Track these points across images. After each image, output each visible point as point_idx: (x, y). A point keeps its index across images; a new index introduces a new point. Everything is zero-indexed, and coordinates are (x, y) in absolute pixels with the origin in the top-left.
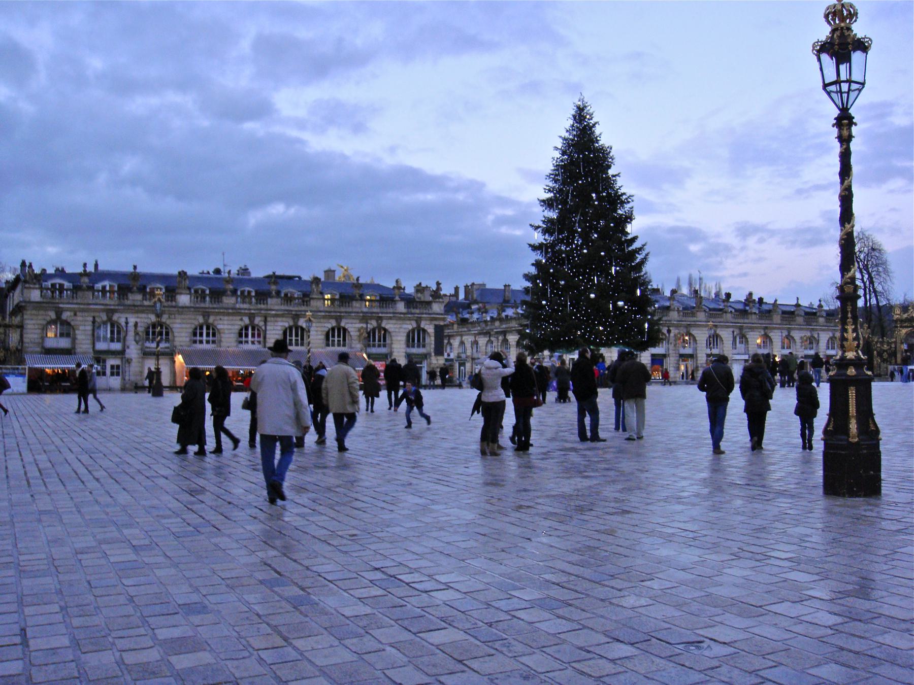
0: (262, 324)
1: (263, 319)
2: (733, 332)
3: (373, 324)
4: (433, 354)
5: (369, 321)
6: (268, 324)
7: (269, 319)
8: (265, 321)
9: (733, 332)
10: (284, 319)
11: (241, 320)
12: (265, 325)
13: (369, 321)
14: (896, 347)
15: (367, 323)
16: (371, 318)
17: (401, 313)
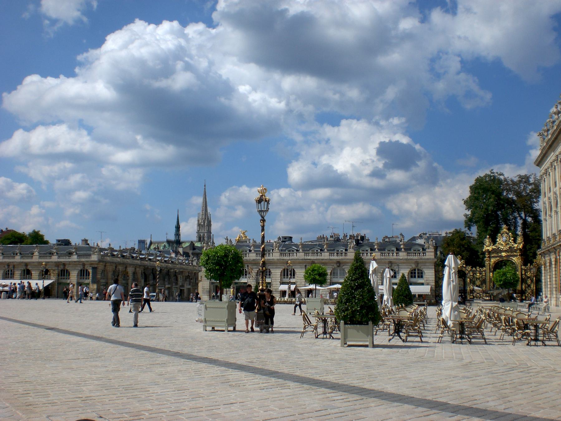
0: (12, 268)
1: (13, 266)
2: (306, 266)
3: (61, 267)
4: (91, 283)
5: (59, 266)
6: (15, 268)
7: (15, 266)
8: (14, 267)
9: (306, 266)
10: (21, 266)
11: (4, 267)
12: (14, 269)
13: (59, 266)
14: (485, 275)
15: (58, 267)
16: (60, 265)
17: (75, 262)
